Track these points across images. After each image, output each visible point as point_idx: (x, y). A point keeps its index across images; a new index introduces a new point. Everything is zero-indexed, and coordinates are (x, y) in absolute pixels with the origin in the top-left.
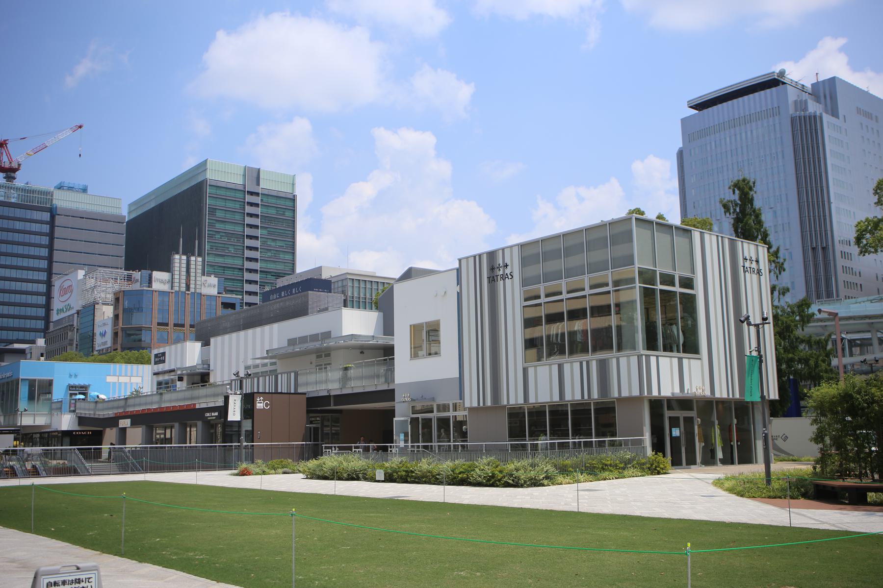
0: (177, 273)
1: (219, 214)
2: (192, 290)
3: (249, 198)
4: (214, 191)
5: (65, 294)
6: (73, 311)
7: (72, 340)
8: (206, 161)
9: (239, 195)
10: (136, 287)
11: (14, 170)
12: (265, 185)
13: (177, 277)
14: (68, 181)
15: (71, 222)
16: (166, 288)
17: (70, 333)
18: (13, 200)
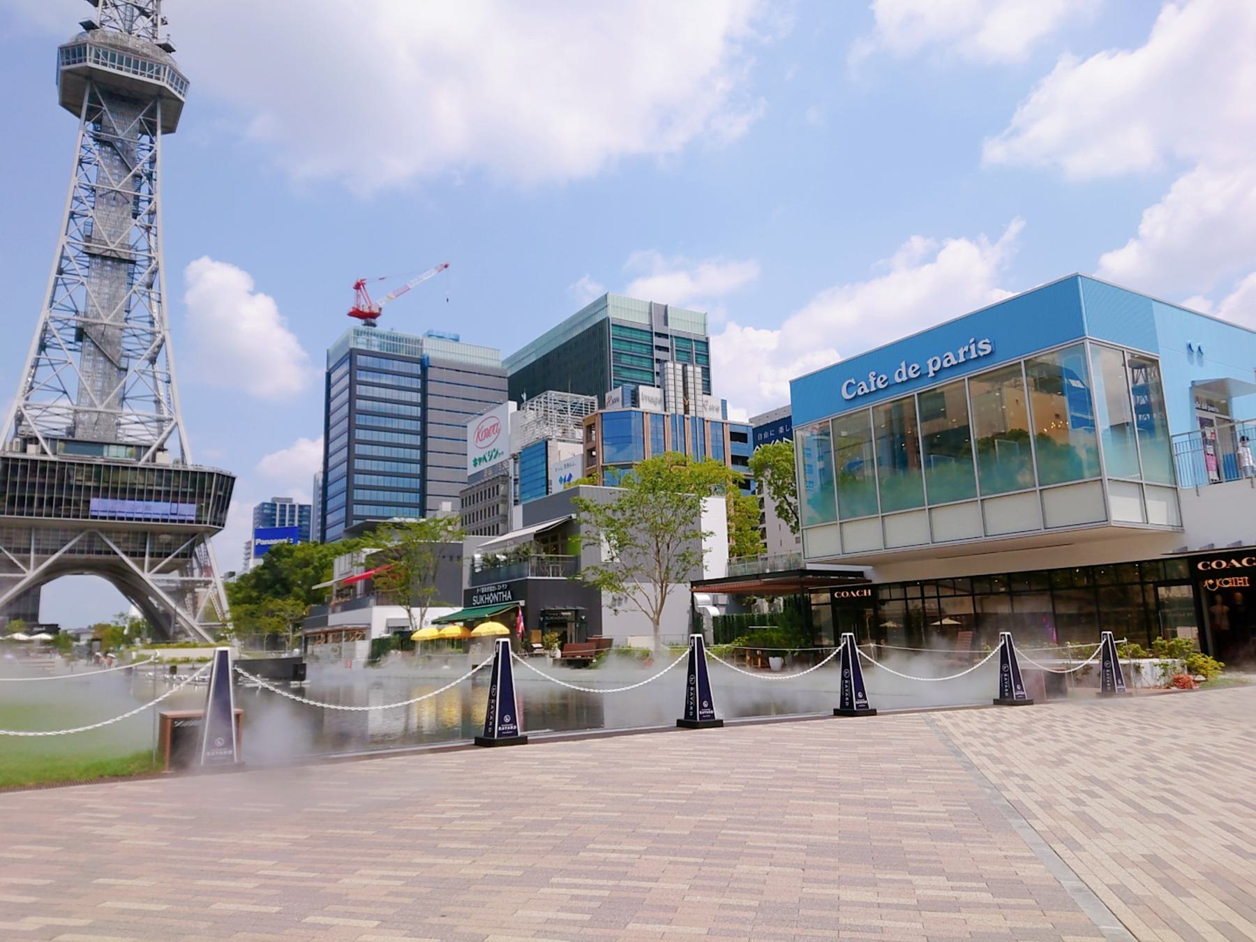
0: (671, 388)
1: (625, 360)
2: (692, 414)
3: (657, 341)
4: (617, 332)
6: (506, 456)
7: (505, 496)
9: (646, 337)
10: (618, 407)
11: (374, 316)
12: (674, 327)
13: (672, 393)
14: (438, 329)
16: (658, 409)
17: (502, 488)
18: (376, 349)
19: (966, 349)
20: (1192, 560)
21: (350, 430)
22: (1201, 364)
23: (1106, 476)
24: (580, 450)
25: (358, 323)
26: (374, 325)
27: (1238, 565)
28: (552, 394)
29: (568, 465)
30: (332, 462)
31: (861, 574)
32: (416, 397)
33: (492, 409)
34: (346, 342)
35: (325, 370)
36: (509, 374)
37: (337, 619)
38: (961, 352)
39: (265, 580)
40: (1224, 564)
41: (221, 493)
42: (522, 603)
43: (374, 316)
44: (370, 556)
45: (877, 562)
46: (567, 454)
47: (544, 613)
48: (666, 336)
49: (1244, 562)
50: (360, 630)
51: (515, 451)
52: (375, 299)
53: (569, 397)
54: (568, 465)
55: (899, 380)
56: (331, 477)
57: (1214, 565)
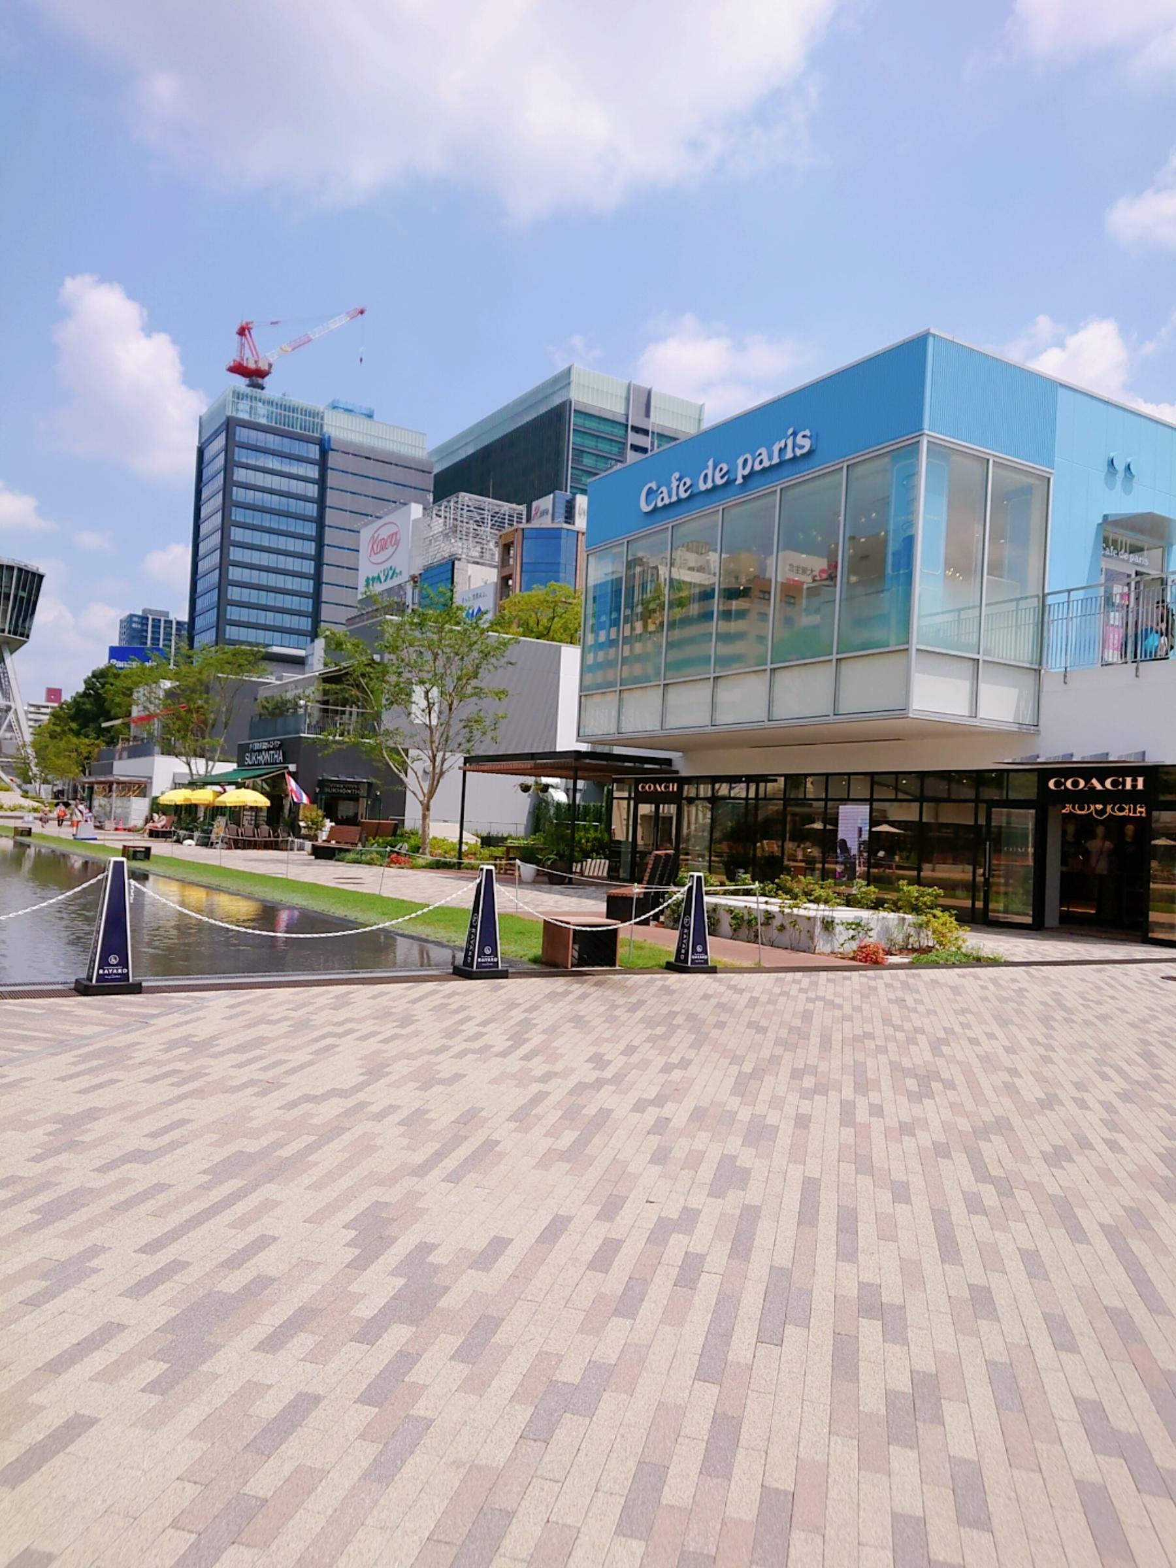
1: (588, 461)
3: (633, 438)
4: (580, 421)
5: (384, 548)
8: (569, 370)
9: (619, 432)
10: (546, 522)
11: (262, 374)
12: (659, 420)
14: (345, 400)
15: (351, 464)
18: (263, 421)
19: (782, 445)
20: (1044, 774)
21: (224, 529)
22: (1128, 489)
23: (915, 645)
24: (491, 576)
25: (241, 382)
26: (263, 388)
27: (1099, 787)
28: (465, 497)
29: (477, 596)
30: (203, 566)
31: (669, 762)
32: (312, 490)
33: (394, 510)
34: (223, 406)
35: (196, 444)
36: (436, 470)
37: (124, 768)
38: (776, 448)
39: (86, 711)
40: (1082, 783)
41: (25, 595)
42: (292, 767)
43: (262, 374)
44: (170, 694)
45: (691, 745)
46: (477, 579)
47: (322, 783)
48: (646, 432)
49: (1108, 783)
50: (139, 784)
51: (417, 573)
52: (265, 350)
53: (489, 503)
54: (477, 596)
55: (703, 487)
56: (200, 587)
57: (1069, 784)
